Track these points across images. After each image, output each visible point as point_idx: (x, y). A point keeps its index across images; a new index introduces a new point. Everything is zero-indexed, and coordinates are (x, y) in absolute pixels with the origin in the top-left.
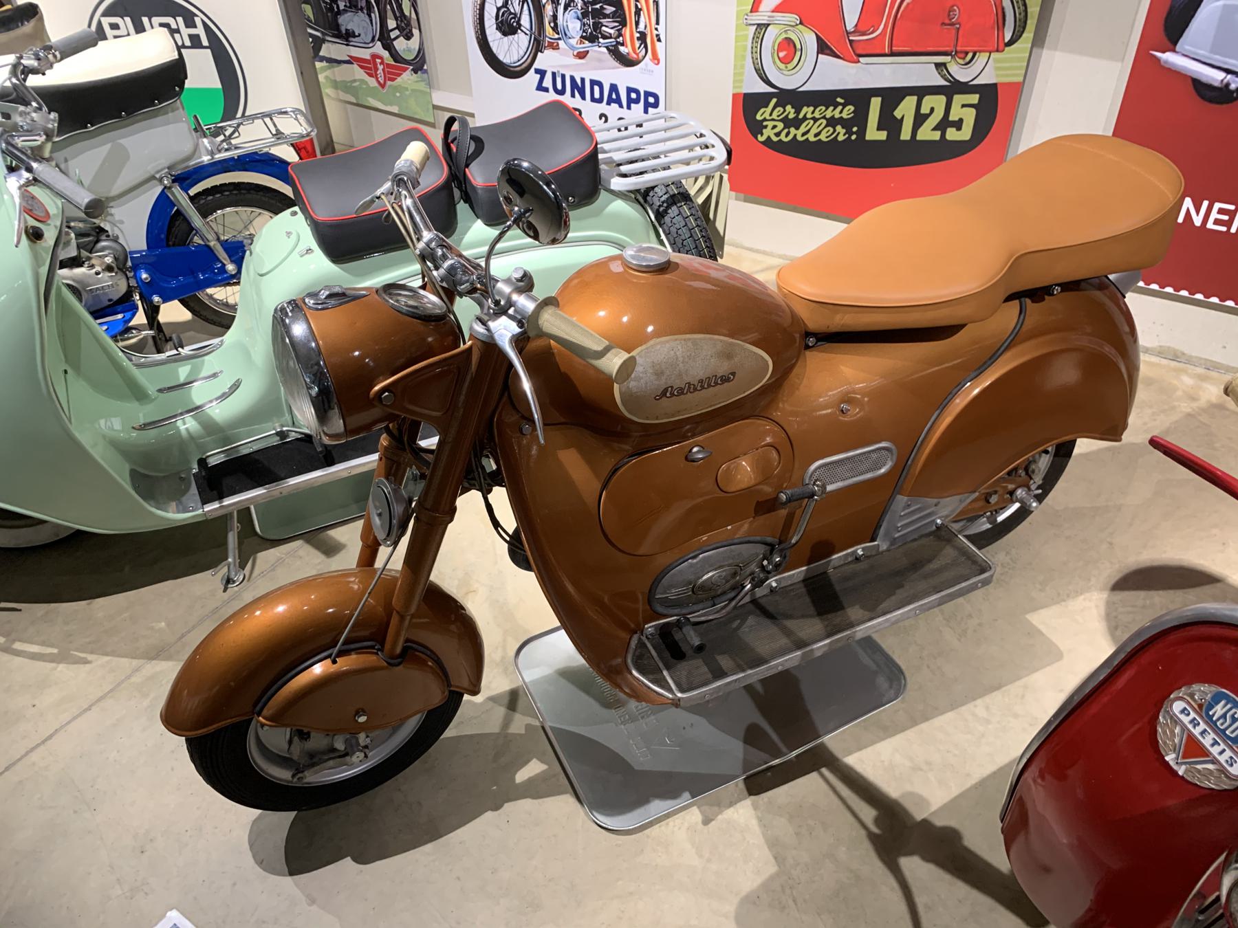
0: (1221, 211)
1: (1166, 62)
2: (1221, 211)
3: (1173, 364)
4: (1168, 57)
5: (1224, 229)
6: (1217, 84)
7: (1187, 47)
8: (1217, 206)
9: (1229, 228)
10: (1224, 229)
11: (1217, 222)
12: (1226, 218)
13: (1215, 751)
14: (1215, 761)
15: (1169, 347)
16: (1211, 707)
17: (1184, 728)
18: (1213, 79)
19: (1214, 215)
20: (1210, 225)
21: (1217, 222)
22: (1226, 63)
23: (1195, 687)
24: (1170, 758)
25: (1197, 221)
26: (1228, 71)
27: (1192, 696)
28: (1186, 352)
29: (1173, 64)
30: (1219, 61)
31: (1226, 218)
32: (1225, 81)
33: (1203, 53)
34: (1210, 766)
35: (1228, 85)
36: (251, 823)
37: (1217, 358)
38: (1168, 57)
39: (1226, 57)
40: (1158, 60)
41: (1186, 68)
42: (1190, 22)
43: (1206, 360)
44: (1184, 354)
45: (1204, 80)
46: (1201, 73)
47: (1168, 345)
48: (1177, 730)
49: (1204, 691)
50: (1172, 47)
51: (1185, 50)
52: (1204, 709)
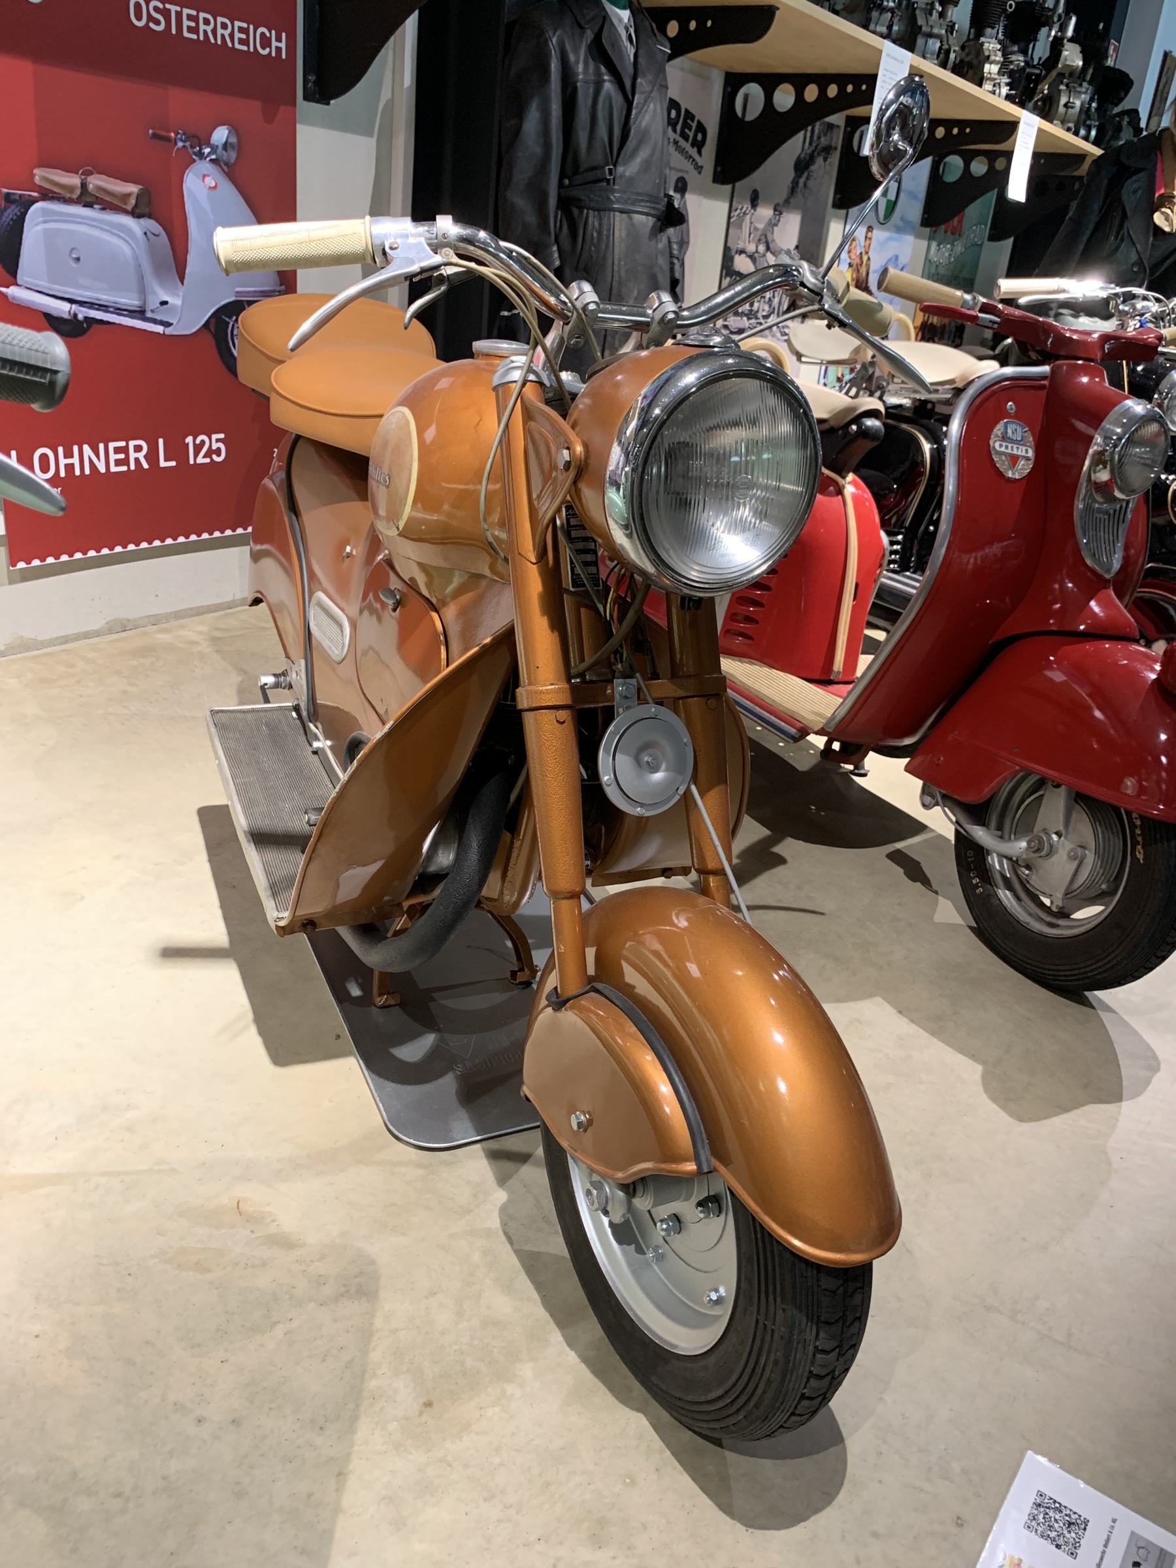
0: (117, 450)
1: (14, 298)
2: (117, 450)
3: (124, 634)
4: (12, 291)
5: (124, 468)
6: (66, 316)
7: (26, 279)
8: (112, 445)
9: (128, 466)
10: (124, 468)
11: (118, 463)
12: (122, 456)
13: (1019, 453)
14: (1024, 457)
15: (115, 620)
16: (1006, 433)
17: (1003, 453)
18: (62, 311)
19: (113, 457)
20: (113, 469)
21: (118, 463)
22: (66, 292)
23: (995, 430)
24: (1010, 474)
25: (102, 469)
26: (71, 301)
27: (997, 436)
28: (130, 617)
29: (20, 299)
30: (59, 291)
31: (122, 456)
32: (72, 312)
33: (44, 284)
34: (1022, 462)
35: (75, 315)
36: (750, 1530)
37: (154, 611)
38: (12, 291)
39: (65, 285)
40: (5, 296)
41: (33, 302)
42: (20, 250)
43: (148, 616)
44: (129, 620)
45: (54, 313)
46: (48, 306)
47: (113, 618)
48: (1004, 458)
49: (998, 429)
50: (12, 279)
51: (26, 282)
52: (1004, 438)
